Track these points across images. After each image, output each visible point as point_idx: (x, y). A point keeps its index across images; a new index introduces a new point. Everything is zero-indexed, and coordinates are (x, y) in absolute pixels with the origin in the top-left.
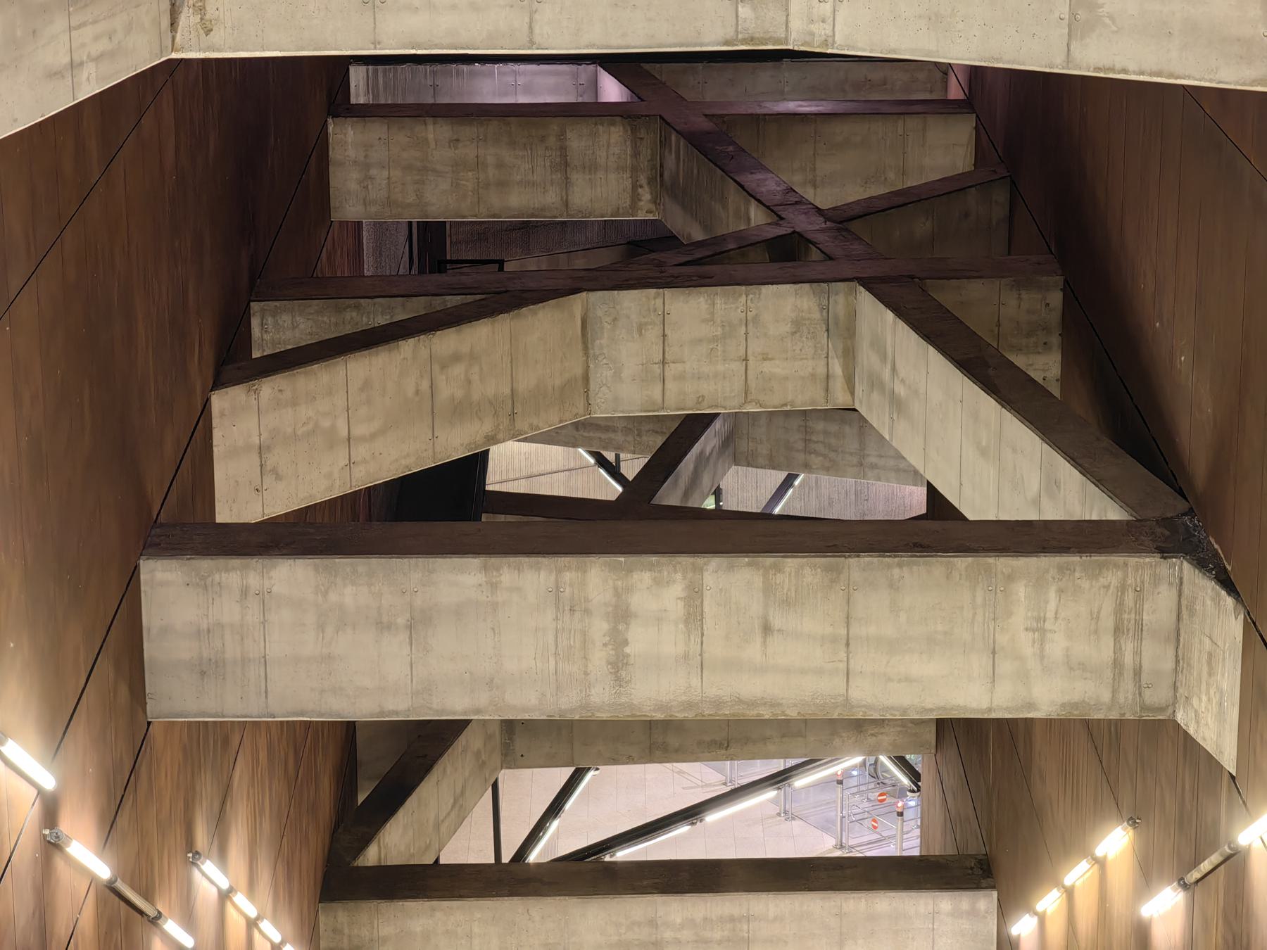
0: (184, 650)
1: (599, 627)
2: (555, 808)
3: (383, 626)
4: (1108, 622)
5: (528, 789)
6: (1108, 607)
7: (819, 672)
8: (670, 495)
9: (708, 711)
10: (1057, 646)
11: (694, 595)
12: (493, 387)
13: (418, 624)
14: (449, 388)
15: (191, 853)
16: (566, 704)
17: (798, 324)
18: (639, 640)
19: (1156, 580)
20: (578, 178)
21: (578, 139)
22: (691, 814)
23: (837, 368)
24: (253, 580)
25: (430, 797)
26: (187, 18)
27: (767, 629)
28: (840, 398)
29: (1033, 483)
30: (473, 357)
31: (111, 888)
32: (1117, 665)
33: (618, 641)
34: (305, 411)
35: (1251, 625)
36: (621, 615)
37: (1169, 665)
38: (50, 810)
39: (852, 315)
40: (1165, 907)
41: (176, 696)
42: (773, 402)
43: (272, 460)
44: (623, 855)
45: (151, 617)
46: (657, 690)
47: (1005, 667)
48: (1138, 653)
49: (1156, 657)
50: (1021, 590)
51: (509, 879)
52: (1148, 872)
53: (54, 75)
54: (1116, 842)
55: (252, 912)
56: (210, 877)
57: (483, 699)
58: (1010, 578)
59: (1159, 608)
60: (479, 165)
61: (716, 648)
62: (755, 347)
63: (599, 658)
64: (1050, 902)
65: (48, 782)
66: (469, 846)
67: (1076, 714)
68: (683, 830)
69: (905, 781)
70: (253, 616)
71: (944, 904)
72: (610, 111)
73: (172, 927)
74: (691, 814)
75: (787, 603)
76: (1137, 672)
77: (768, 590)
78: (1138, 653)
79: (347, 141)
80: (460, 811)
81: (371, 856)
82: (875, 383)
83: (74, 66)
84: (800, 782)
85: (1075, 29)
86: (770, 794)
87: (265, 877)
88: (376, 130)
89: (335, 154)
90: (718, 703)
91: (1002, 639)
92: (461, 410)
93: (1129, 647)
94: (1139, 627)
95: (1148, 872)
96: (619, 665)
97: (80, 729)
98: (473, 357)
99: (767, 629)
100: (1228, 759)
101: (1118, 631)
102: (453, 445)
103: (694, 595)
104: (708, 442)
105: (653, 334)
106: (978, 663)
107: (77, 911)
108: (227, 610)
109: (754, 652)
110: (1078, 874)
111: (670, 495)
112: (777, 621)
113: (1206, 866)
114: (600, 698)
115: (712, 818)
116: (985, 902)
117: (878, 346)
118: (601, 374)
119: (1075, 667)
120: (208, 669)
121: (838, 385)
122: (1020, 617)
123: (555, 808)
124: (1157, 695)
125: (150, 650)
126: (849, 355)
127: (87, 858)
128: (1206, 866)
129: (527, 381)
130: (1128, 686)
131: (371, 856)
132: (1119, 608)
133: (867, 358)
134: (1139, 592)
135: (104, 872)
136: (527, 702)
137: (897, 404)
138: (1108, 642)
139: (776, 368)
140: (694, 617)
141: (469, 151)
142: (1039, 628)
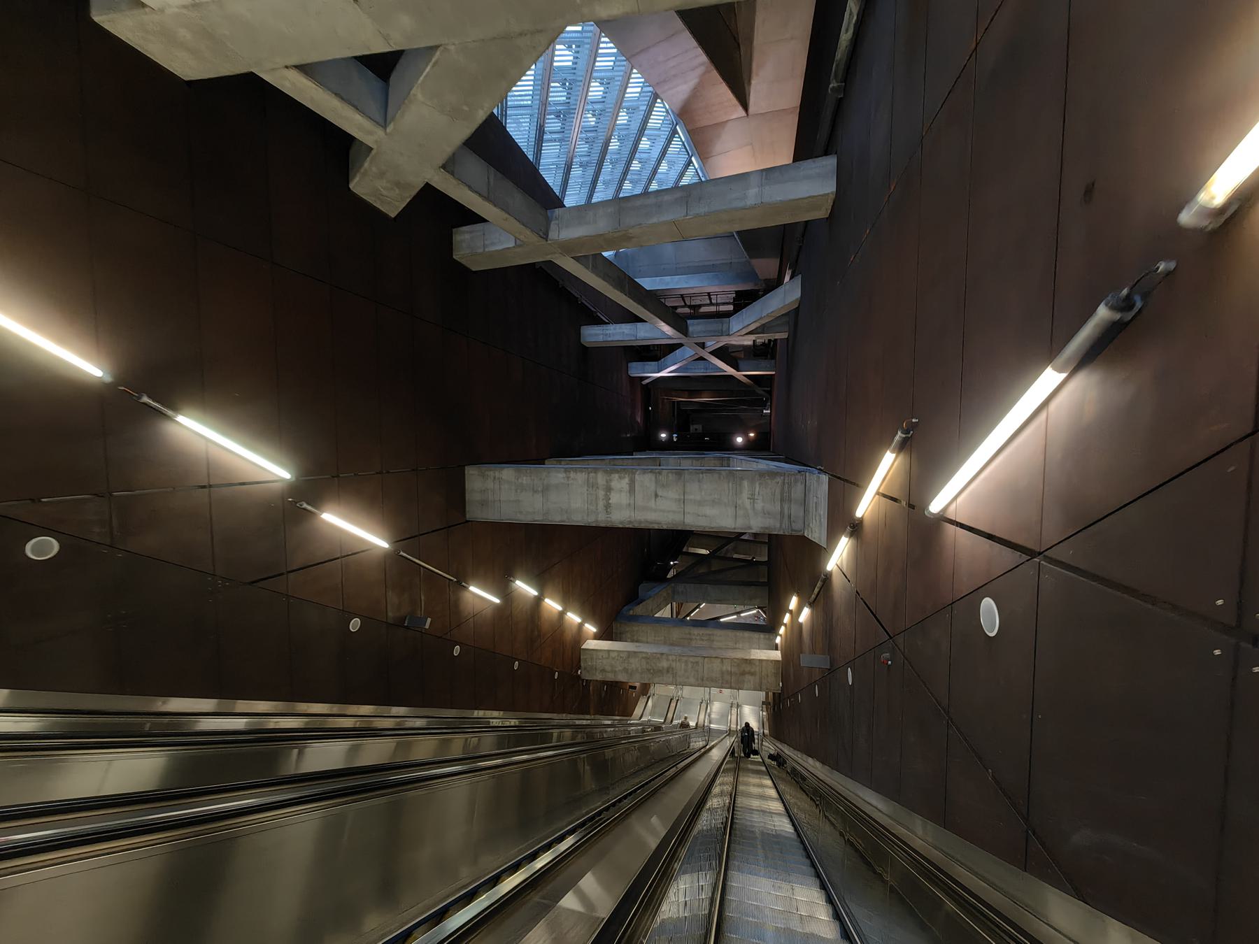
1: (601, 493)
3: (535, 491)
4: (778, 496)
7: (674, 512)
9: (637, 525)
10: (759, 505)
13: (546, 489)
18: (615, 498)
19: (796, 481)
24: (497, 474)
25: (649, 604)
27: (656, 496)
32: (782, 513)
33: (607, 498)
36: (609, 489)
37: (802, 514)
41: (475, 512)
47: (740, 512)
48: (789, 509)
49: (796, 511)
50: (745, 483)
55: (560, 608)
57: (565, 518)
58: (742, 479)
59: (798, 491)
63: (601, 504)
64: (782, 630)
67: (767, 532)
71: (762, 636)
75: (663, 486)
76: (790, 517)
77: (656, 482)
78: (789, 509)
90: (640, 522)
91: (739, 502)
93: (786, 507)
96: (608, 506)
99: (656, 496)
106: (731, 511)
108: (490, 484)
109: (652, 504)
112: (660, 493)
113: (816, 590)
119: (766, 513)
120: (484, 503)
122: (745, 494)
124: (798, 526)
125: (467, 496)
128: (816, 590)
132: (782, 494)
134: (790, 485)
136: (578, 519)
140: (632, 490)
142: (752, 498)
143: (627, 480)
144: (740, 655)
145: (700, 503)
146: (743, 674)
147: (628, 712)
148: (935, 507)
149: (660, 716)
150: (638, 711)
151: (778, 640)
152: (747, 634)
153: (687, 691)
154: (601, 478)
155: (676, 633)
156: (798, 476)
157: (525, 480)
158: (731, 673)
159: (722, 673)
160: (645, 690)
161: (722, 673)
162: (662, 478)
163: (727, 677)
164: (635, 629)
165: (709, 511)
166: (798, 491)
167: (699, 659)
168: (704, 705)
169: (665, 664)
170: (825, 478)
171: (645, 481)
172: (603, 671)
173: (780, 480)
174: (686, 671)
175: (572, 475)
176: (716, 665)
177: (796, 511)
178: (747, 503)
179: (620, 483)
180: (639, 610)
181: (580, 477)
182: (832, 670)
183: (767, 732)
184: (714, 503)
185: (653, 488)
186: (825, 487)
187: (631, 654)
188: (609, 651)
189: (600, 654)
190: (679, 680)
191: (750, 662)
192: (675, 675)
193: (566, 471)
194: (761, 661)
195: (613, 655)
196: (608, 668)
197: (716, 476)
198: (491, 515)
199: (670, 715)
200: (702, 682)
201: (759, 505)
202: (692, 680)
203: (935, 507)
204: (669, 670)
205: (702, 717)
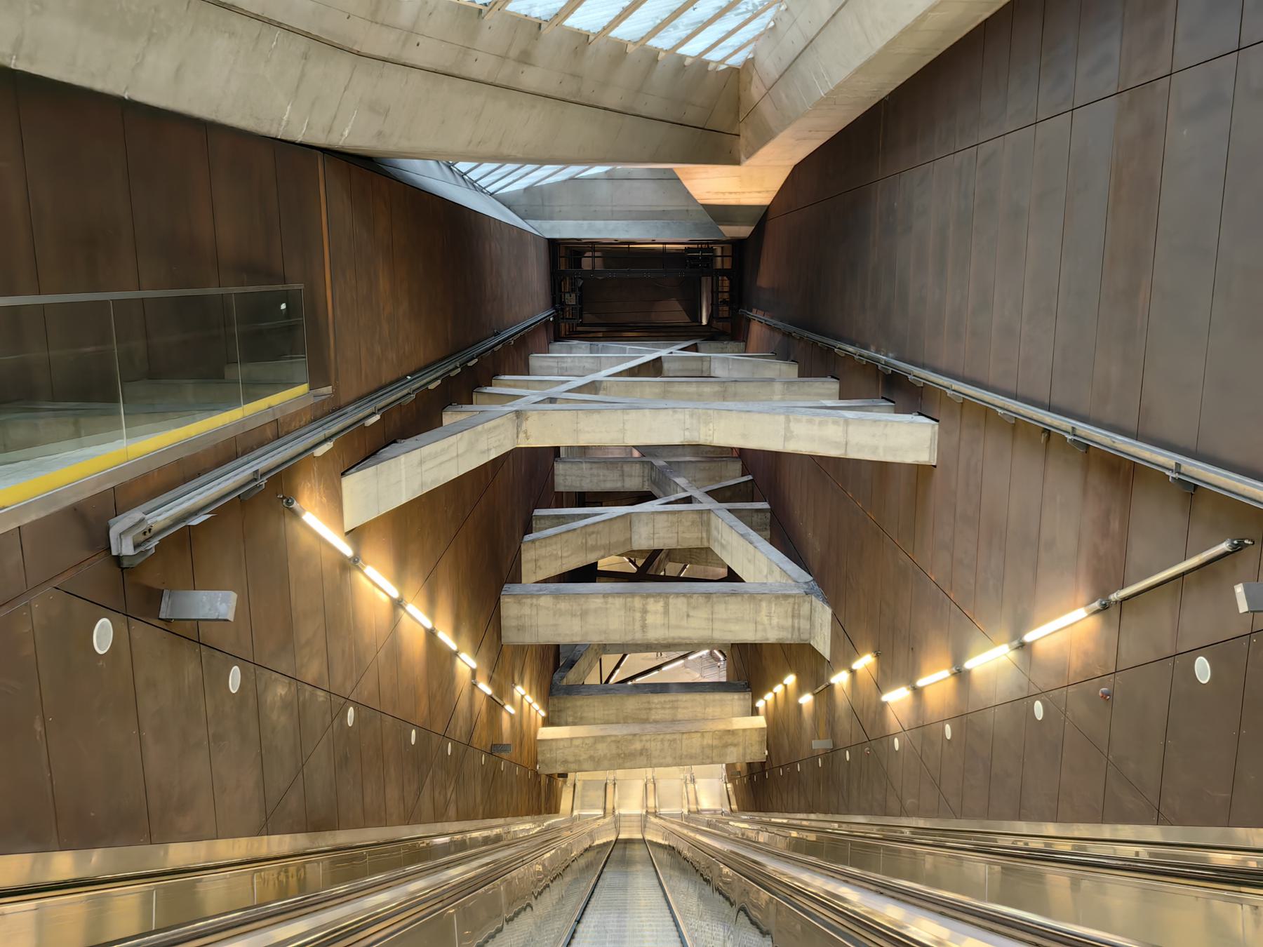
0: (514, 623)
1: (638, 615)
2: (617, 666)
3: (573, 615)
4: (790, 613)
5: (610, 660)
6: (790, 610)
8: (651, 572)
10: (775, 621)
11: (666, 606)
12: (603, 541)
13: (584, 614)
14: (591, 542)
15: (513, 684)
16: (628, 638)
17: (693, 522)
18: (650, 619)
20: (627, 479)
21: (627, 468)
22: (658, 668)
23: (704, 535)
24: (534, 601)
25: (582, 664)
26: (522, 435)
28: (706, 545)
29: (765, 571)
30: (598, 533)
31: (491, 697)
32: (793, 627)
33: (643, 619)
34: (549, 549)
35: (834, 615)
36: (645, 611)
38: (474, 672)
39: (709, 520)
40: (807, 700)
41: (511, 636)
42: (685, 545)
43: (541, 563)
44: (638, 680)
45: (504, 612)
46: (654, 635)
47: (760, 627)
49: (805, 624)
50: (764, 604)
51: (605, 688)
52: (801, 689)
53: (483, 452)
54: (791, 680)
56: (519, 691)
59: (805, 609)
60: (598, 475)
61: (673, 621)
62: (681, 529)
63: (638, 625)
64: (769, 697)
65: (474, 665)
66: (593, 679)
68: (656, 673)
69: (722, 658)
70: (534, 612)
71: (736, 696)
72: (635, 461)
73: (508, 708)
74: (658, 668)
75: (694, 608)
77: (689, 604)
79: (560, 468)
80: (590, 667)
81: (565, 682)
82: (716, 540)
83: (489, 450)
84: (691, 658)
85: (786, 439)
86: (682, 662)
87: (534, 690)
88: (568, 466)
89: (556, 472)
92: (594, 548)
94: (799, 616)
95: (801, 689)
96: (644, 627)
97: (483, 650)
98: (598, 533)
100: (827, 656)
101: (793, 616)
102: (591, 559)
103: (666, 606)
104: (662, 555)
105: (651, 525)
106: (752, 626)
107: (481, 705)
108: (526, 610)
109: (684, 623)
110: (779, 689)
111: (651, 572)
114: (638, 637)
115: (664, 669)
116: (748, 696)
117: (717, 528)
118: (635, 538)
119: (781, 628)
120: (520, 628)
121: (705, 540)
122: (764, 612)
123: (617, 666)
124: (805, 636)
126: (708, 532)
127: (485, 688)
129: (614, 539)
130: (796, 633)
131: (565, 682)
133: (714, 533)
135: (489, 691)
136: (616, 638)
137: (723, 546)
138: (790, 620)
139: (687, 535)
140: (666, 612)
141: (595, 471)
142: (769, 616)
143: (661, 603)
144: (722, 726)
145: (726, 621)
146: (726, 746)
147: (553, 808)
148: (885, 698)
149: (593, 807)
150: (565, 803)
151: (760, 704)
152: (718, 696)
153: (620, 773)
154: (638, 602)
155: (632, 704)
156: (807, 598)
157: (563, 605)
158: (712, 747)
159: (703, 748)
160: (564, 776)
161: (703, 748)
162: (693, 601)
163: (708, 752)
164: (579, 703)
165: (735, 627)
166: (805, 609)
167: (677, 736)
168: (650, 786)
169: (638, 746)
170: (828, 611)
171: (678, 604)
172: (565, 762)
173: (791, 600)
174: (662, 750)
175: (610, 600)
176: (696, 741)
177: (805, 624)
178: (765, 620)
179: (655, 606)
180: (571, 677)
181: (619, 602)
182: (834, 750)
183: (734, 807)
184: (738, 620)
185: (685, 609)
186: (830, 617)
187: (598, 739)
188: (571, 739)
189: (561, 744)
190: (654, 761)
191: (732, 733)
192: (649, 757)
193: (605, 595)
194: (744, 730)
195: (576, 742)
196: (571, 759)
197: (739, 599)
198: (528, 639)
199: (609, 806)
200: (680, 761)
201: (775, 621)
202: (669, 760)
203: (885, 698)
204: (643, 752)
205: (651, 803)
